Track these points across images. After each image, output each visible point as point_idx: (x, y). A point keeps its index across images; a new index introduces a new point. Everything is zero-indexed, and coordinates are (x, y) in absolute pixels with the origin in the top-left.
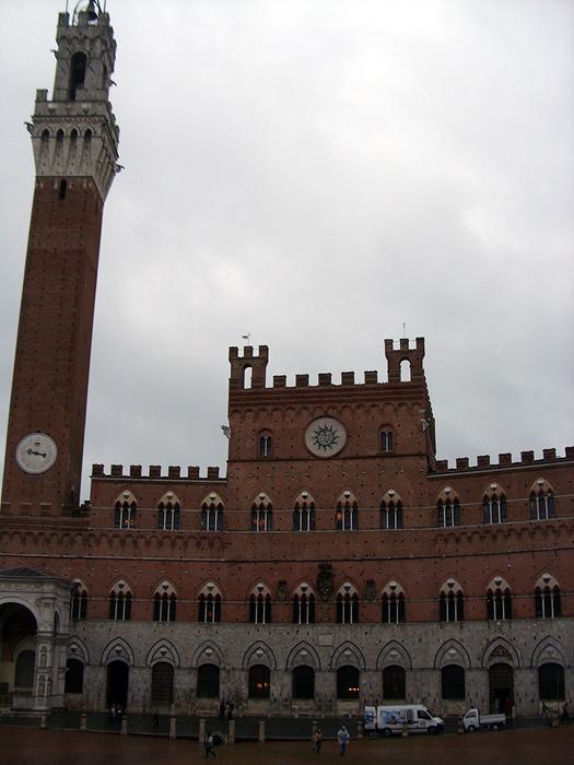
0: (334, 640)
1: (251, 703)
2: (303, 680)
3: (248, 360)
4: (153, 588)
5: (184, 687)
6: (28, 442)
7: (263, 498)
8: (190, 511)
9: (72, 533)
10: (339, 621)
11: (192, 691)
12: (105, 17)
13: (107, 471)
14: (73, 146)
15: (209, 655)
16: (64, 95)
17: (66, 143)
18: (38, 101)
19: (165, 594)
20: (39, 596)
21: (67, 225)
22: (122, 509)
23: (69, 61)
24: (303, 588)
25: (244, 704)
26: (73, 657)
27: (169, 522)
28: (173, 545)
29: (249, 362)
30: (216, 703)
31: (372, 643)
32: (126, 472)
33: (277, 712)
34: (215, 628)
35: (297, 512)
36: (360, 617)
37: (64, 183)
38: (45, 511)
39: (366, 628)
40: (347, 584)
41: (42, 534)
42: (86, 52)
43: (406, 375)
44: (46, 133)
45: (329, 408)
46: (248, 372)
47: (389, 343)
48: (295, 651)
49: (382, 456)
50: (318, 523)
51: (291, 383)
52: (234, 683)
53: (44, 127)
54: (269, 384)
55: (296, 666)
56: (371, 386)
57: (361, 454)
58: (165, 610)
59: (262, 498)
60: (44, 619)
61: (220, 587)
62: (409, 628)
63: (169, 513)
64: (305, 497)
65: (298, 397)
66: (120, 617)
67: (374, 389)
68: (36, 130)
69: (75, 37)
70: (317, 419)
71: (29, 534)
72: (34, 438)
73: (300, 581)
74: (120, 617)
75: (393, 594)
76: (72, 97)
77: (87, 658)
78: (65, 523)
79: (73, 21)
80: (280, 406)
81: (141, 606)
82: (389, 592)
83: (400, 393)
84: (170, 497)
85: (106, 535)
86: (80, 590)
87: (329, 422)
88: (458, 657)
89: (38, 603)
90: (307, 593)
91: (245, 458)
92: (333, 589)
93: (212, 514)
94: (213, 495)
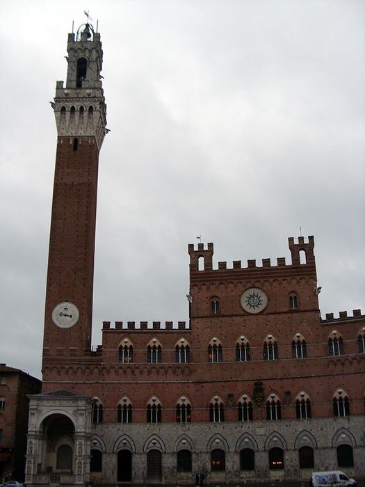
0: (266, 430)
1: (213, 474)
2: (247, 458)
3: (200, 252)
4: (146, 401)
5: (169, 465)
6: (59, 308)
7: (216, 341)
8: (168, 351)
9: (91, 367)
10: (268, 418)
11: (174, 467)
12: (97, 36)
13: (113, 326)
14: (81, 117)
15: (184, 444)
16: (74, 84)
17: (77, 114)
18: (57, 88)
19: (341, 397)
20: (75, 409)
21: (77, 166)
22: (123, 350)
23: (76, 63)
24: (244, 398)
25: (209, 475)
26: (95, 448)
27: (154, 358)
28: (158, 373)
29: (202, 253)
30: (190, 475)
31: (291, 432)
32: (125, 326)
33: (231, 480)
34: (187, 426)
35: (238, 349)
36: (282, 415)
37: (76, 140)
38: (73, 353)
39: (287, 423)
40: (273, 395)
41: (71, 368)
42: (85, 56)
43: (303, 261)
44: (63, 109)
46: (201, 260)
47: (291, 240)
48: (241, 439)
49: (291, 312)
50: (252, 356)
51: (230, 266)
52: (201, 462)
53: (61, 105)
54: (215, 267)
55: (242, 448)
56: (282, 267)
58: (154, 415)
59: (215, 341)
60: (81, 423)
61: (190, 399)
62: (314, 421)
63: (154, 352)
64: (243, 340)
65: (235, 275)
66: (125, 421)
67: (283, 269)
68: (57, 107)
69: (79, 49)
70: (247, 289)
71: (63, 368)
72: (64, 305)
73: (242, 394)
74: (125, 421)
75: (303, 400)
76: (79, 85)
77: (104, 448)
78: (86, 360)
79: (78, 38)
80: (224, 282)
81: (139, 413)
82: (300, 398)
83: (301, 271)
84: (154, 342)
85: (114, 368)
86: (98, 404)
87: (256, 291)
88: (347, 439)
89: (75, 413)
90: (247, 401)
91: (202, 315)
92: (264, 398)
93: (183, 352)
94: (183, 340)
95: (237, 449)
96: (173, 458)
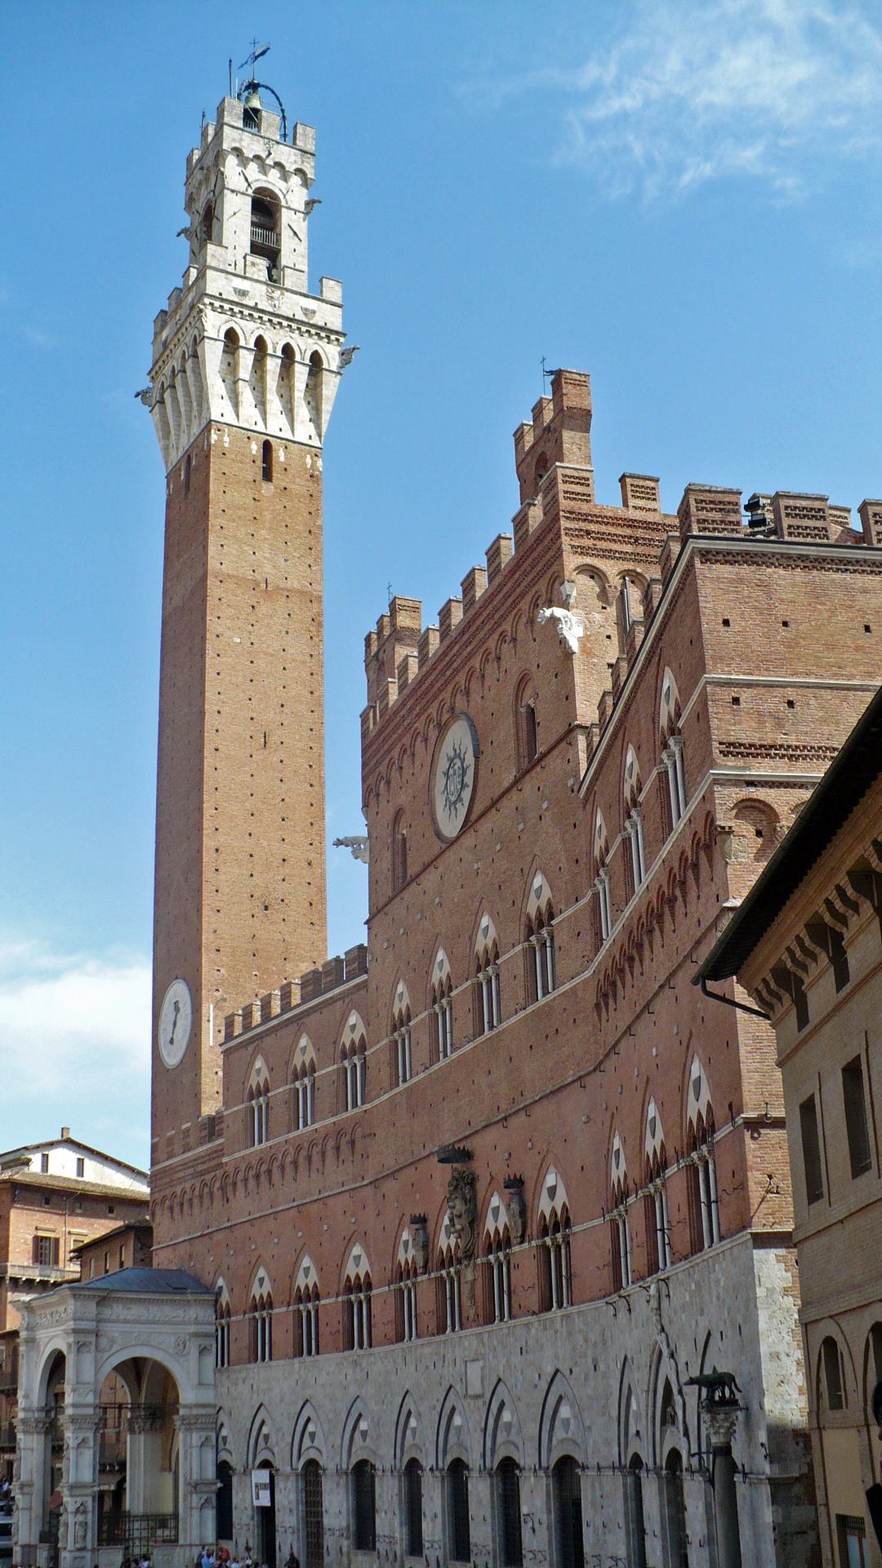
9: (208, 1177)
15: (364, 1434)
26: (224, 1456)
37: (189, 459)
45: (454, 695)
57: (498, 792)
84: (305, 1049)
95: (440, 1465)
96: (342, 1491)
